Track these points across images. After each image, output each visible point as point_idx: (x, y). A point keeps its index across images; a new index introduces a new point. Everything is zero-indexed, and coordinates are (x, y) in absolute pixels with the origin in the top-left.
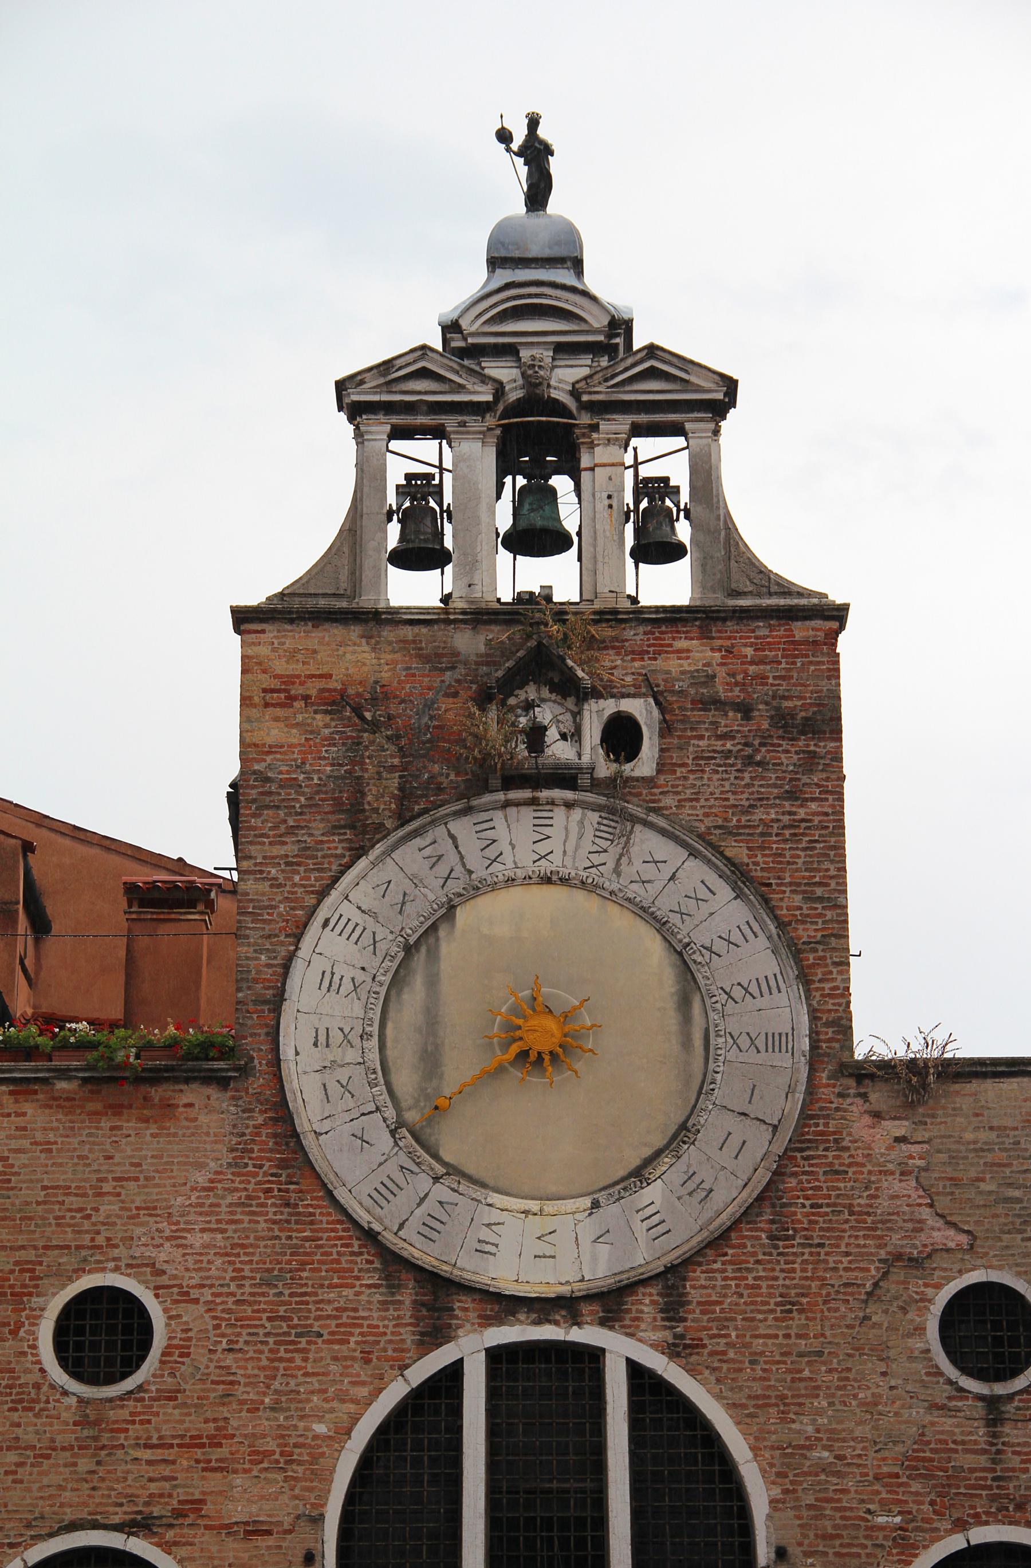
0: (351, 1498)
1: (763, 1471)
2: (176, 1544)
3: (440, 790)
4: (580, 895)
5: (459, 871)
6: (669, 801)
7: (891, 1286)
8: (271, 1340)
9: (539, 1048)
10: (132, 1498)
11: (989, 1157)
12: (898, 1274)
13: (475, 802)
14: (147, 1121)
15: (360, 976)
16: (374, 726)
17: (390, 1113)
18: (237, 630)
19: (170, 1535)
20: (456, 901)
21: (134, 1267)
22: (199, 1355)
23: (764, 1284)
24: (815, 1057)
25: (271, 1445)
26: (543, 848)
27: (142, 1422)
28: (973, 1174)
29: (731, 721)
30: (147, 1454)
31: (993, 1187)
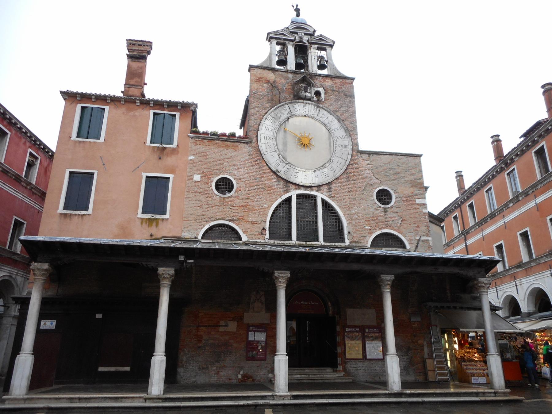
0: (271, 219)
1: (346, 219)
2: (238, 224)
3: (286, 99)
4: (311, 119)
5: (290, 112)
6: (326, 105)
7: (367, 188)
8: (256, 189)
9: (305, 143)
10: (230, 215)
11: (383, 168)
12: (368, 186)
13: (293, 101)
14: (233, 149)
15: (272, 128)
16: (274, 87)
17: (278, 152)
18: (249, 71)
19: (237, 222)
20: (289, 118)
21: (230, 174)
22: (243, 191)
23: (345, 187)
24: (353, 150)
25: (256, 208)
26: (305, 110)
27: (232, 202)
28: (380, 170)
29: (337, 94)
30: (233, 208)
31: (384, 173)
